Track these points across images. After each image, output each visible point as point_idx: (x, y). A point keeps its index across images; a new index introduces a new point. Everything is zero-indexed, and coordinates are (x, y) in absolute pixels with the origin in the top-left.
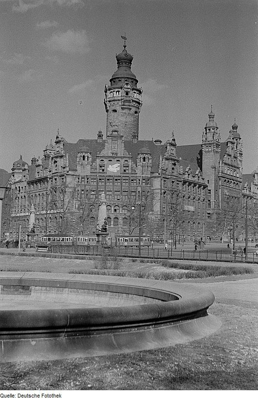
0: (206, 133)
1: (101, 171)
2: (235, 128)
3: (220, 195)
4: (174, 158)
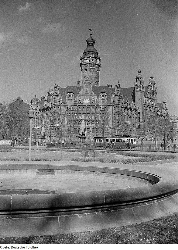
0: (136, 81)
1: (80, 103)
2: (152, 78)
3: (145, 114)
4: (120, 95)
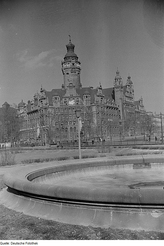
1: (65, 104)
2: (129, 78)
4: (102, 95)
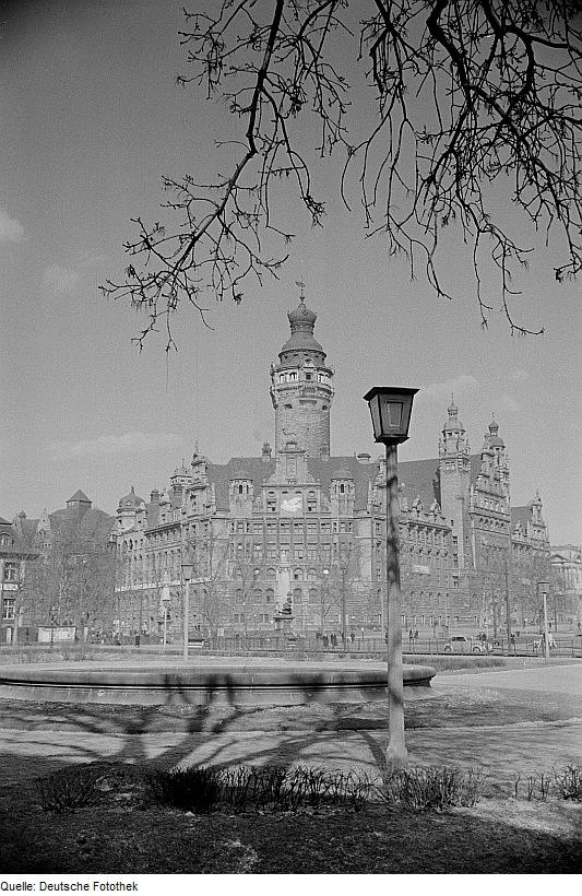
2: (494, 429)
